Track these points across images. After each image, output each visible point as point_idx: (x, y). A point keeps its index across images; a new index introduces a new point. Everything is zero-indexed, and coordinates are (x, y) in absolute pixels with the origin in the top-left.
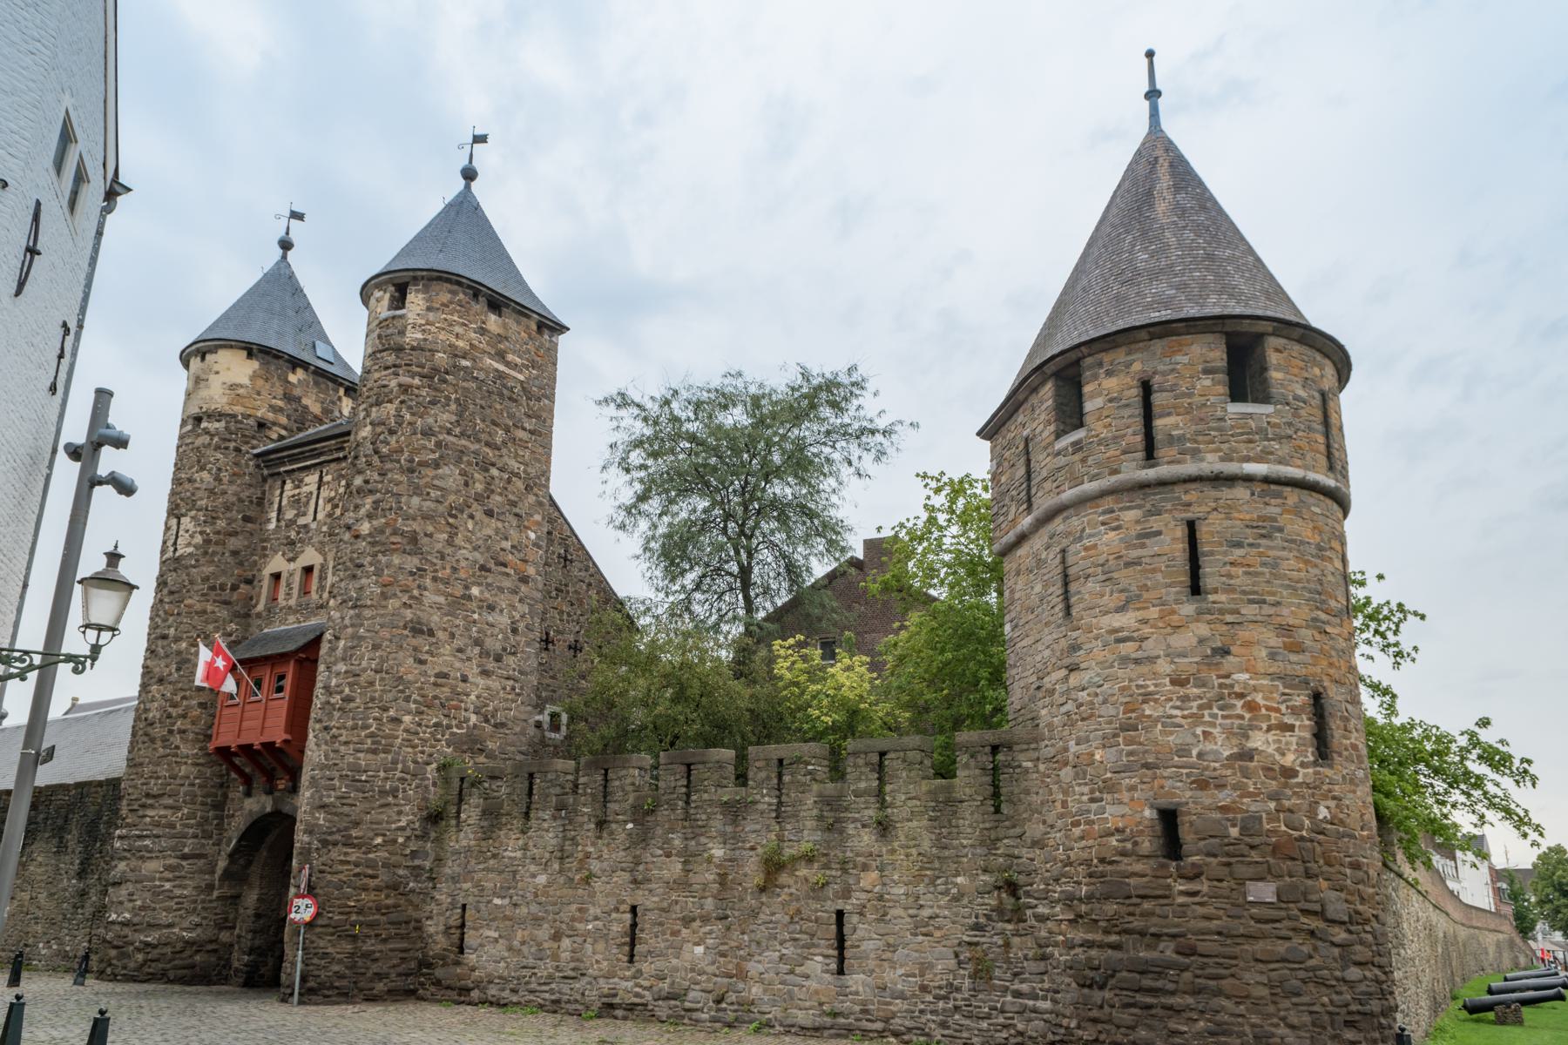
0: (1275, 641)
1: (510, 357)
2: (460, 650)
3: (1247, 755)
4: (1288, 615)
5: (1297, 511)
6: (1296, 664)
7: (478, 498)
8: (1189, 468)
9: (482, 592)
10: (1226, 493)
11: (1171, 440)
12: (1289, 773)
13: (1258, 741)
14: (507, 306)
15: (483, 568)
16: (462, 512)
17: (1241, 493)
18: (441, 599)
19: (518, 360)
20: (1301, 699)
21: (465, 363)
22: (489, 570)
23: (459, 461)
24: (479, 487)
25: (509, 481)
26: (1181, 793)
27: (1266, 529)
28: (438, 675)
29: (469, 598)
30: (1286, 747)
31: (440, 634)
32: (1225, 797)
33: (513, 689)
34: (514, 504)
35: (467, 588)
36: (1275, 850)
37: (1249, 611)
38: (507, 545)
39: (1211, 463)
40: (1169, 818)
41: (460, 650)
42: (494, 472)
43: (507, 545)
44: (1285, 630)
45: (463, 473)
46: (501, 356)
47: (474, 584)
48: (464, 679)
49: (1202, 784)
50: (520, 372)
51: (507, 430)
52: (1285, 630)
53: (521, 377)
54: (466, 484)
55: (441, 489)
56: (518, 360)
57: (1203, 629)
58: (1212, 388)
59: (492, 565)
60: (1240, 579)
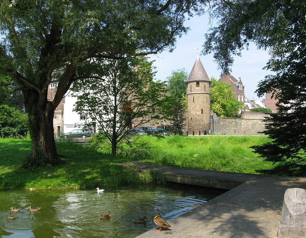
0: (199, 106)
3: (196, 114)
4: (200, 104)
5: (201, 95)
6: (201, 107)
8: (193, 93)
10: (196, 94)
11: (193, 90)
12: (199, 115)
13: (197, 113)
17: (197, 94)
20: (201, 110)
26: (192, 117)
27: (199, 97)
30: (200, 113)
32: (195, 117)
36: (198, 120)
37: (197, 103)
39: (195, 92)
40: (192, 118)
44: (200, 105)
49: (194, 116)
52: (200, 105)
57: (194, 105)
58: (195, 86)
60: (197, 101)
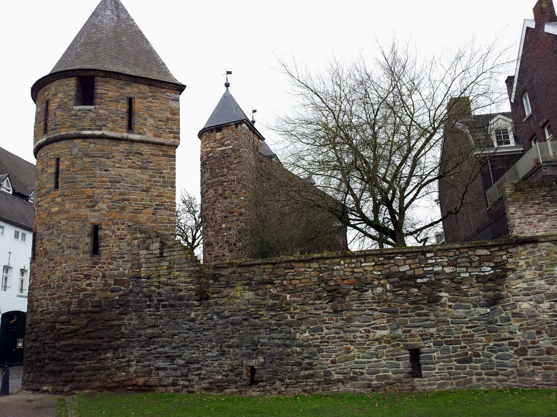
1: (226, 143)
2: (221, 247)
7: (221, 195)
9: (226, 225)
14: (223, 127)
15: (226, 217)
16: (216, 202)
18: (213, 233)
19: (229, 142)
21: (210, 155)
22: (228, 217)
23: (213, 186)
24: (220, 192)
25: (231, 184)
28: (215, 257)
29: (222, 229)
31: (215, 244)
33: (242, 253)
34: (234, 191)
35: (221, 226)
38: (233, 206)
41: (221, 247)
42: (225, 184)
43: (233, 206)
45: (215, 190)
46: (223, 145)
47: (223, 223)
48: (224, 255)
50: (231, 145)
51: (228, 167)
53: (231, 147)
54: (216, 193)
55: (209, 198)
56: (229, 142)
59: (229, 215)
